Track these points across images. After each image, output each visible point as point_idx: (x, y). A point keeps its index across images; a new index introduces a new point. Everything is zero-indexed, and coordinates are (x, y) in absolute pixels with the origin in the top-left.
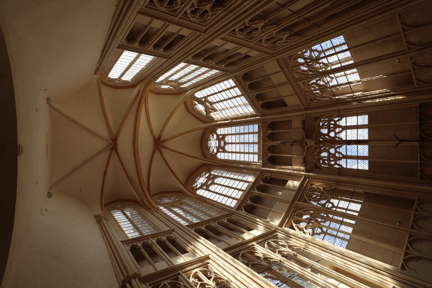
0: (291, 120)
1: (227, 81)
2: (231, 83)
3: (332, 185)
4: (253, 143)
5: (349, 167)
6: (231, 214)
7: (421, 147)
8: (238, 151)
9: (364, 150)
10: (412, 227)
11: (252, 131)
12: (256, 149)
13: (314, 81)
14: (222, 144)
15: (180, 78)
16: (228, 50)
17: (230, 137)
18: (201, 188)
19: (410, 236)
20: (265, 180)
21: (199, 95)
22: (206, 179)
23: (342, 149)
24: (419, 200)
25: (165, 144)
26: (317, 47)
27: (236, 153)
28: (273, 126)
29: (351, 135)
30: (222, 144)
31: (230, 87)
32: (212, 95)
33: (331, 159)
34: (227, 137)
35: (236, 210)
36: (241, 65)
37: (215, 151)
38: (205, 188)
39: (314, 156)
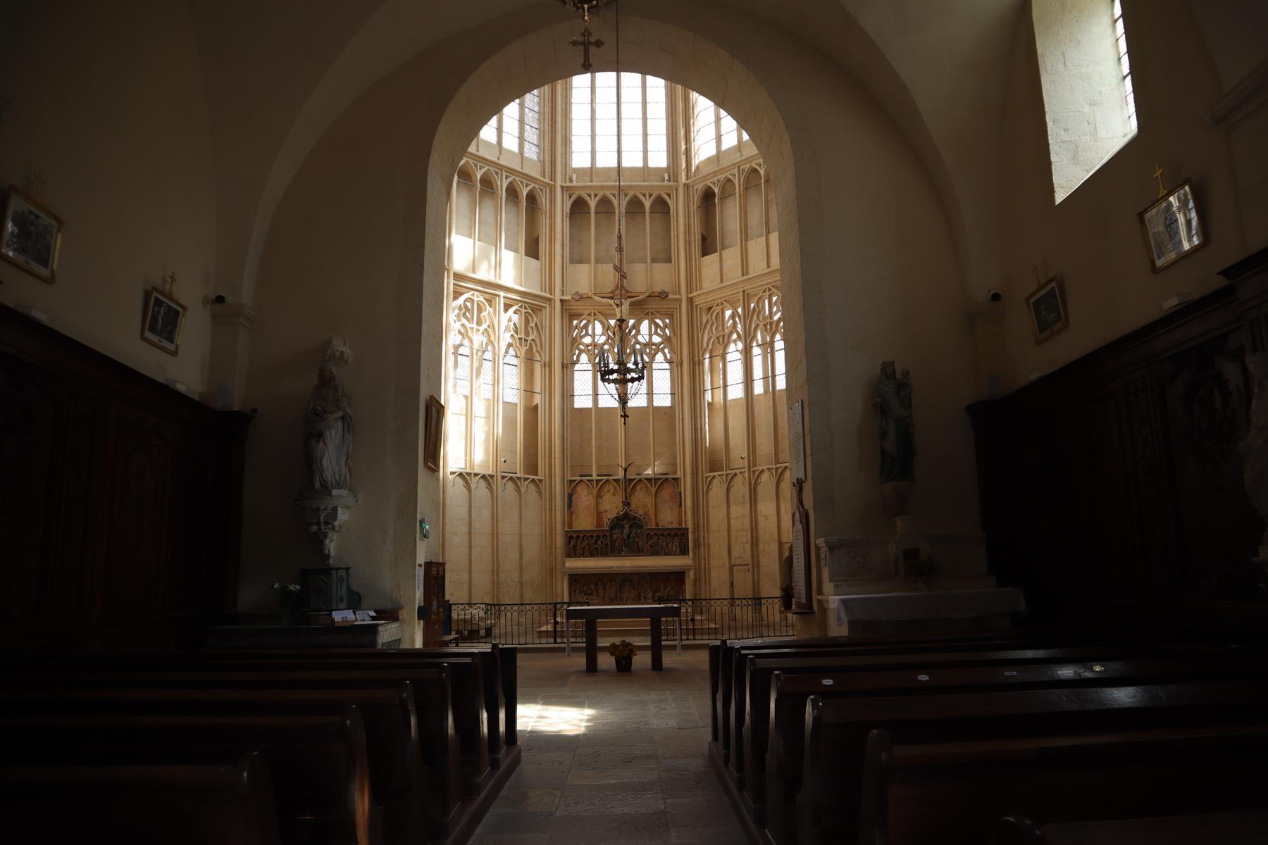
0: (669, 261)
7: (617, 481)
10: (503, 477)
12: (607, 160)
19: (492, 476)
20: (532, 198)
24: (540, 481)
28: (661, 206)
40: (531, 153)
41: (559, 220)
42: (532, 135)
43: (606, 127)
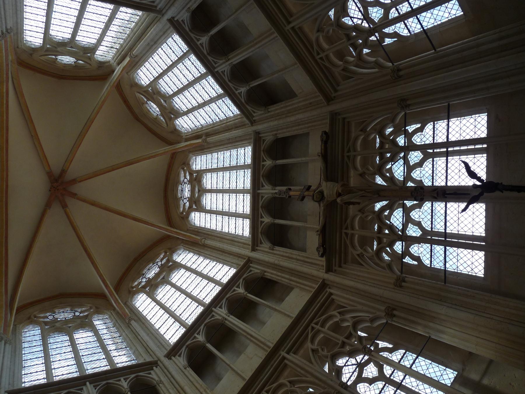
3: (378, 313)
23: (422, 214)
25: (77, 189)
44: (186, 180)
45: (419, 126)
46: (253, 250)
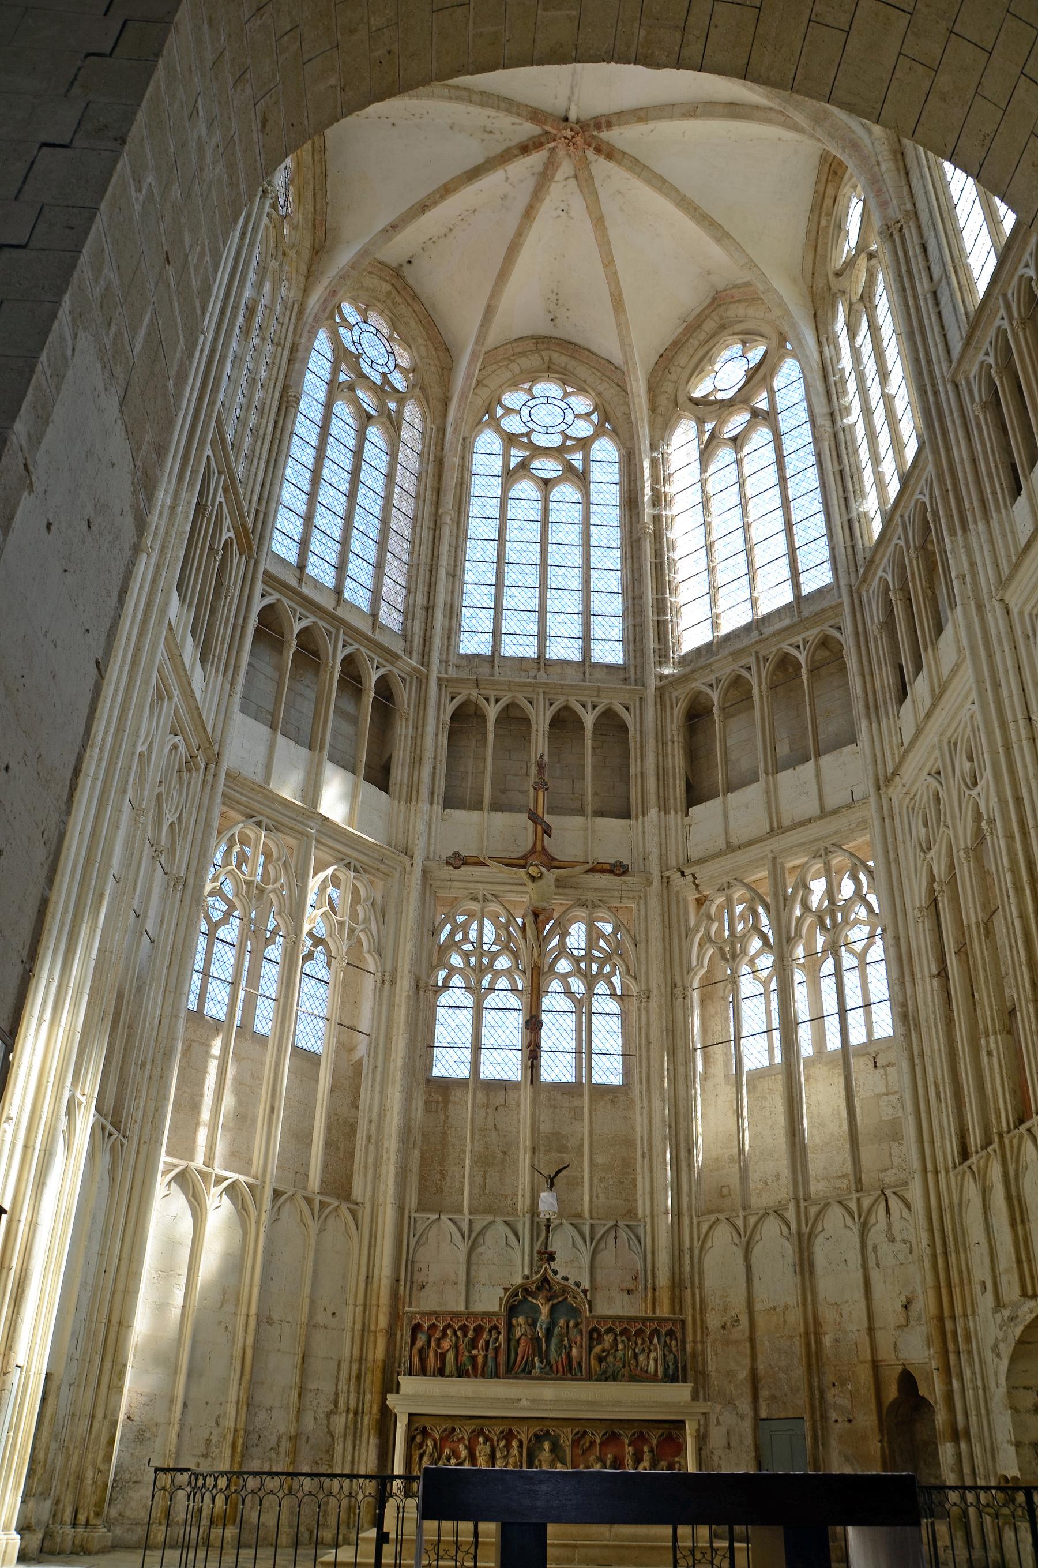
1: (826, 554)
2: (817, 577)
4: (542, 636)
5: (441, 1013)
6: (250, 548)
8: (511, 556)
9: (503, 1065)
11: (596, 632)
12: (519, 646)
13: (764, 920)
14: (546, 467)
15: (874, 329)
16: (939, 629)
17: (576, 513)
18: (342, 356)
21: (790, 383)
22: (377, 379)
26: (877, 951)
27: (501, 541)
28: (612, 725)
29: (558, 1031)
30: (546, 467)
31: (801, 567)
32: (780, 461)
33: (473, 960)
34: (577, 496)
35: (266, 572)
36: (880, 648)
37: (512, 425)
38: (343, 377)
39: (485, 899)
40: (391, 618)
41: (430, 729)
42: (393, 590)
43: (521, 599)
44: (572, 416)
45: (619, 992)
46: (439, 679)
